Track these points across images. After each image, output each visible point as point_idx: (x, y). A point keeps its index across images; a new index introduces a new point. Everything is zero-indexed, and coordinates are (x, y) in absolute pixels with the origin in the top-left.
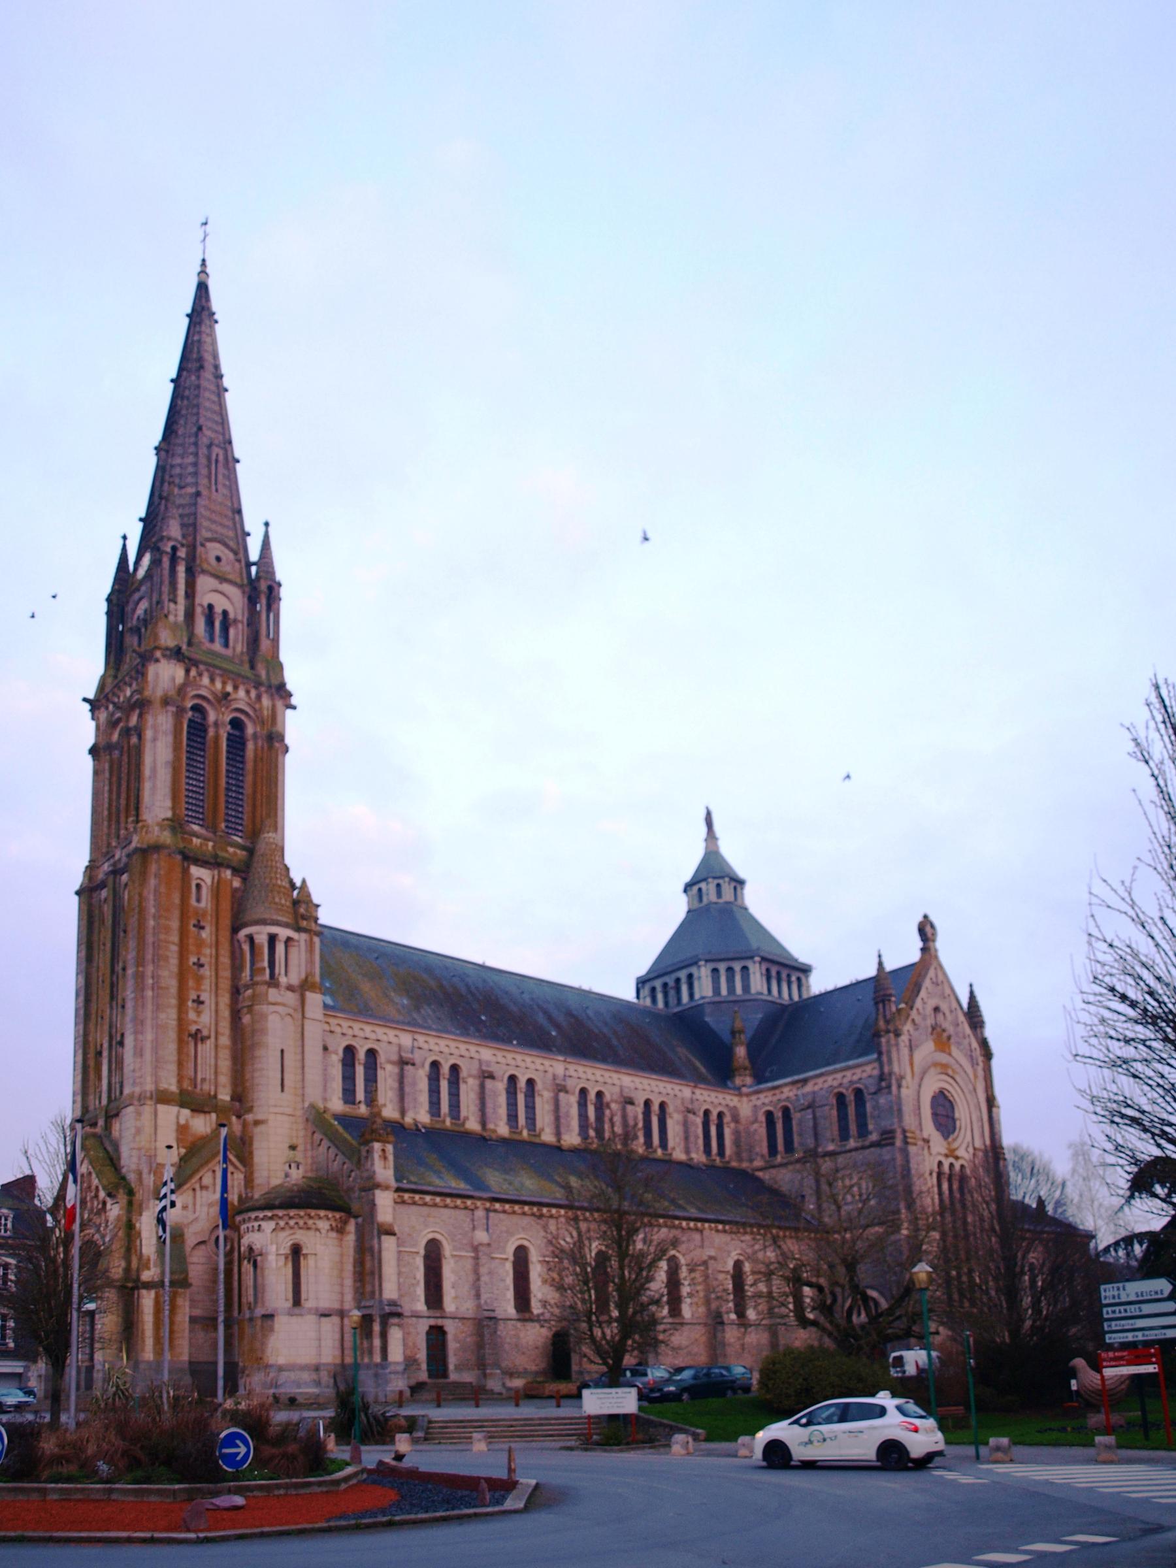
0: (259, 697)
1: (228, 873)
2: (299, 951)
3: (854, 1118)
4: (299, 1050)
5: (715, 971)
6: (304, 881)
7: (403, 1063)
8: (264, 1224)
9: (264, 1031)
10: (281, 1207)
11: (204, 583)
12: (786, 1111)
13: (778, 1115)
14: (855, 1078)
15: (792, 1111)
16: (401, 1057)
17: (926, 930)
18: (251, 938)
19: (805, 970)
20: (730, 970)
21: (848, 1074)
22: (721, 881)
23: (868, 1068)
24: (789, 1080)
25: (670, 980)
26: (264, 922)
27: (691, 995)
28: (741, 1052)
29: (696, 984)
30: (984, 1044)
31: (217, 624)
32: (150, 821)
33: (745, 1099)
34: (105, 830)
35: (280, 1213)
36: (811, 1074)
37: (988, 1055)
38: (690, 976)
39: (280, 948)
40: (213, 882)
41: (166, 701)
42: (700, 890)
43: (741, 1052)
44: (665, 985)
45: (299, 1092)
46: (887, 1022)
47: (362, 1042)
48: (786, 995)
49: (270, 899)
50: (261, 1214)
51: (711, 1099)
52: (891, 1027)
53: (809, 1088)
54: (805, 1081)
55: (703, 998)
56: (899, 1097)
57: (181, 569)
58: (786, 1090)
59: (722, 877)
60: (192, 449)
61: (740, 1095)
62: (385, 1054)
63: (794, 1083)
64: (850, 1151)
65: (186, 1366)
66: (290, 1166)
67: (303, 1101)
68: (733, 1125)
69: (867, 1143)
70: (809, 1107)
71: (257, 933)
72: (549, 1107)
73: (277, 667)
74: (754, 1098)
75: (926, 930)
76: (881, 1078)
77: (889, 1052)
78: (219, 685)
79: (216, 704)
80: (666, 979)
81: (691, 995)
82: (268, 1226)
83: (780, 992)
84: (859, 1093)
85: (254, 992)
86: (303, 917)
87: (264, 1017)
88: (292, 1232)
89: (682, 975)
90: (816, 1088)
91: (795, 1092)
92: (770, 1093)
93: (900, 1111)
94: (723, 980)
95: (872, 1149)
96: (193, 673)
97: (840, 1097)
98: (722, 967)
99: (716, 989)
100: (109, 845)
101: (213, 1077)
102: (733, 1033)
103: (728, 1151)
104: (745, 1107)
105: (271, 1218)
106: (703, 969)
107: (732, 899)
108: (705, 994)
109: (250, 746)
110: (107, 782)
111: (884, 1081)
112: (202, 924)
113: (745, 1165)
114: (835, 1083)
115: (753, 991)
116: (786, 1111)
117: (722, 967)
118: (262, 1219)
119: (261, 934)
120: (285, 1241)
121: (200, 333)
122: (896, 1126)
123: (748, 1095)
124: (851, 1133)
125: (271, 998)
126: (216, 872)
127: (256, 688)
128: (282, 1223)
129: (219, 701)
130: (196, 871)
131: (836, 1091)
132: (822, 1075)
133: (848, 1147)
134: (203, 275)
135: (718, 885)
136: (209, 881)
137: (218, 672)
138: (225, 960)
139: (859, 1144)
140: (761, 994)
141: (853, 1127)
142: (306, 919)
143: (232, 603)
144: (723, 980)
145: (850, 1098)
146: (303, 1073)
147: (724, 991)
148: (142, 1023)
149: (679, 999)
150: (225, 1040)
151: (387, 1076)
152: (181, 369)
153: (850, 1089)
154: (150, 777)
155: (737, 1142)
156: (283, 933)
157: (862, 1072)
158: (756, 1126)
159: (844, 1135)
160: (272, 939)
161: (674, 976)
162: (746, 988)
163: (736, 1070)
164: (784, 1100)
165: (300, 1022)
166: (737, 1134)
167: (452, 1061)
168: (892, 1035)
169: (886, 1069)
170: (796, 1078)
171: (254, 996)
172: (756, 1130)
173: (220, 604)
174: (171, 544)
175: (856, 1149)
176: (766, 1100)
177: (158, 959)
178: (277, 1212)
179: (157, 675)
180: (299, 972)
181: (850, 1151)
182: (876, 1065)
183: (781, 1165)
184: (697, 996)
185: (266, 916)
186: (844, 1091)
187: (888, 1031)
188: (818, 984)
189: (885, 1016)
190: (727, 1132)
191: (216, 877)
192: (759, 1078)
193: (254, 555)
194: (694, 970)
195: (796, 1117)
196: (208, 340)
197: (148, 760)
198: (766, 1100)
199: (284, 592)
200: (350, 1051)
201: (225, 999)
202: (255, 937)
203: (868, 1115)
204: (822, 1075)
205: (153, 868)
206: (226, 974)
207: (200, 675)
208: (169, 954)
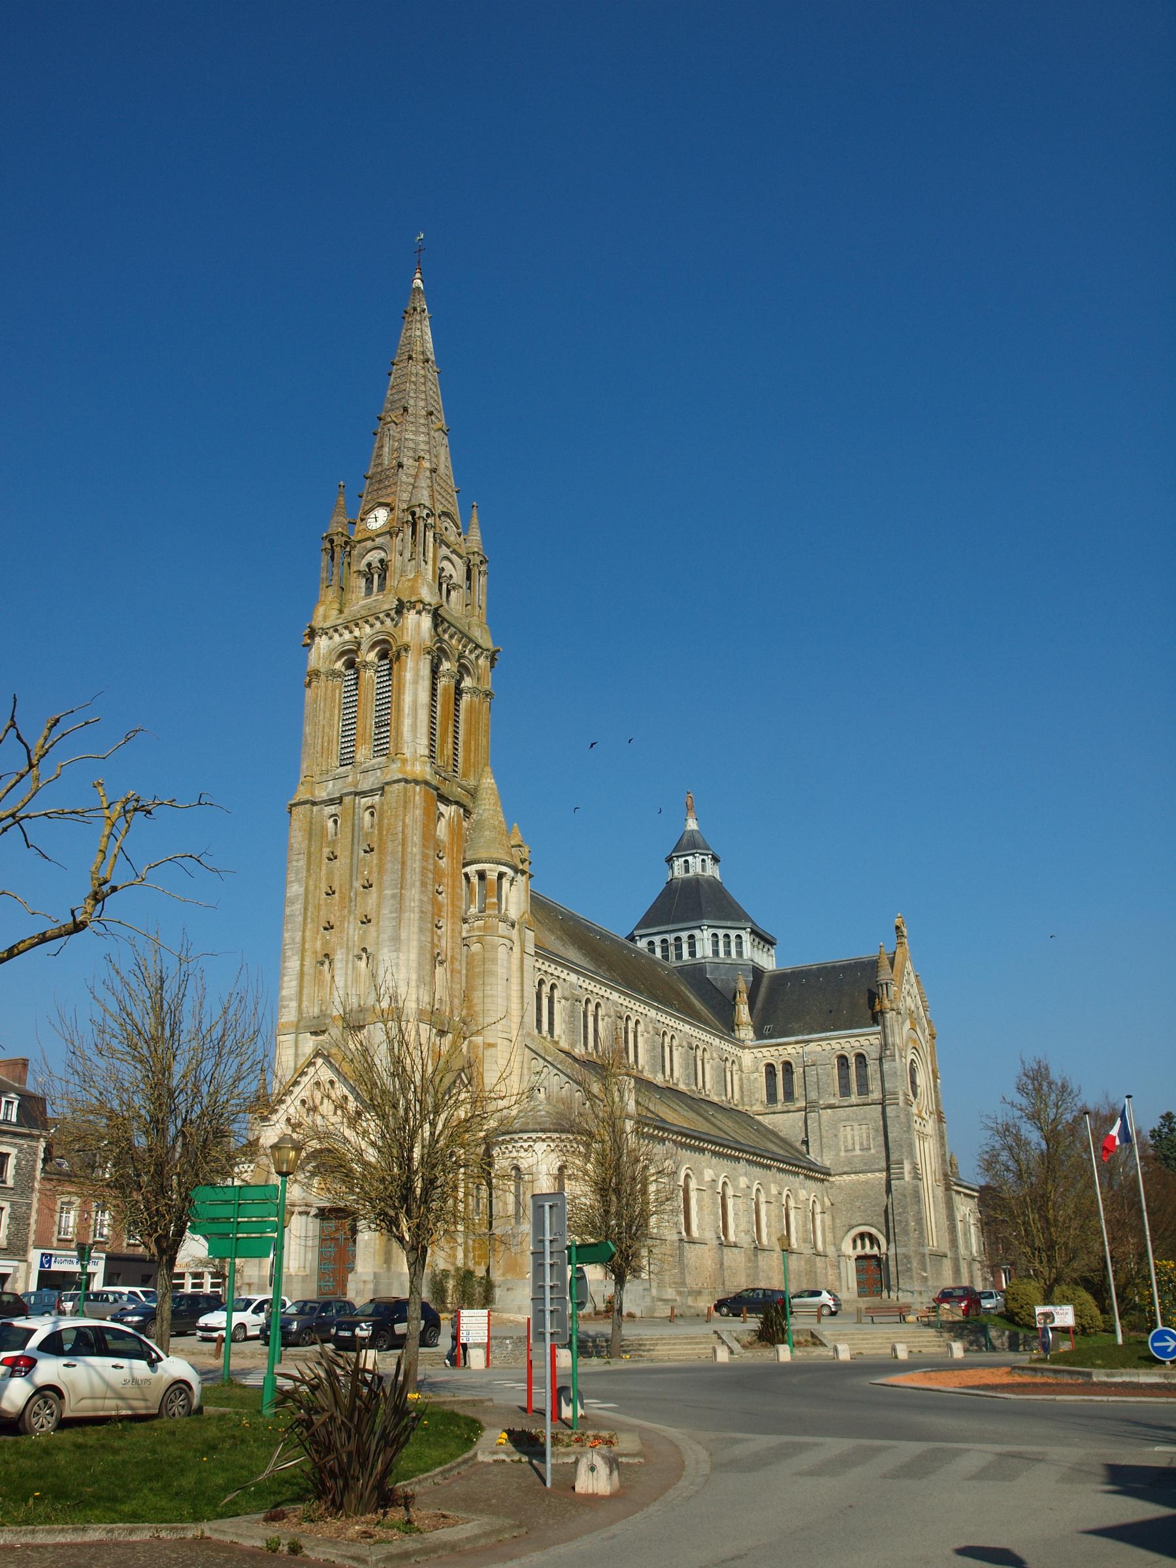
5: (715, 935)
12: (787, 1066)
15: (794, 1066)
20: (727, 936)
22: (705, 857)
27: (692, 954)
29: (698, 945)
35: (555, 1135)
38: (691, 937)
42: (686, 862)
50: (534, 1135)
54: (808, 1042)
55: (704, 958)
58: (789, 1048)
81: (692, 954)
89: (684, 935)
97: (843, 1059)
98: (721, 933)
105: (544, 1140)
108: (706, 955)
115: (745, 957)
116: (787, 1066)
131: (839, 1053)
135: (703, 860)
139: (859, 1101)
145: (852, 1060)
147: (722, 954)
149: (679, 956)
159: (845, 1090)
162: (740, 954)
166: (741, 1079)
170: (800, 1038)
178: (549, 1135)
184: (698, 955)
186: (846, 1054)
194: (696, 932)
195: (798, 1071)
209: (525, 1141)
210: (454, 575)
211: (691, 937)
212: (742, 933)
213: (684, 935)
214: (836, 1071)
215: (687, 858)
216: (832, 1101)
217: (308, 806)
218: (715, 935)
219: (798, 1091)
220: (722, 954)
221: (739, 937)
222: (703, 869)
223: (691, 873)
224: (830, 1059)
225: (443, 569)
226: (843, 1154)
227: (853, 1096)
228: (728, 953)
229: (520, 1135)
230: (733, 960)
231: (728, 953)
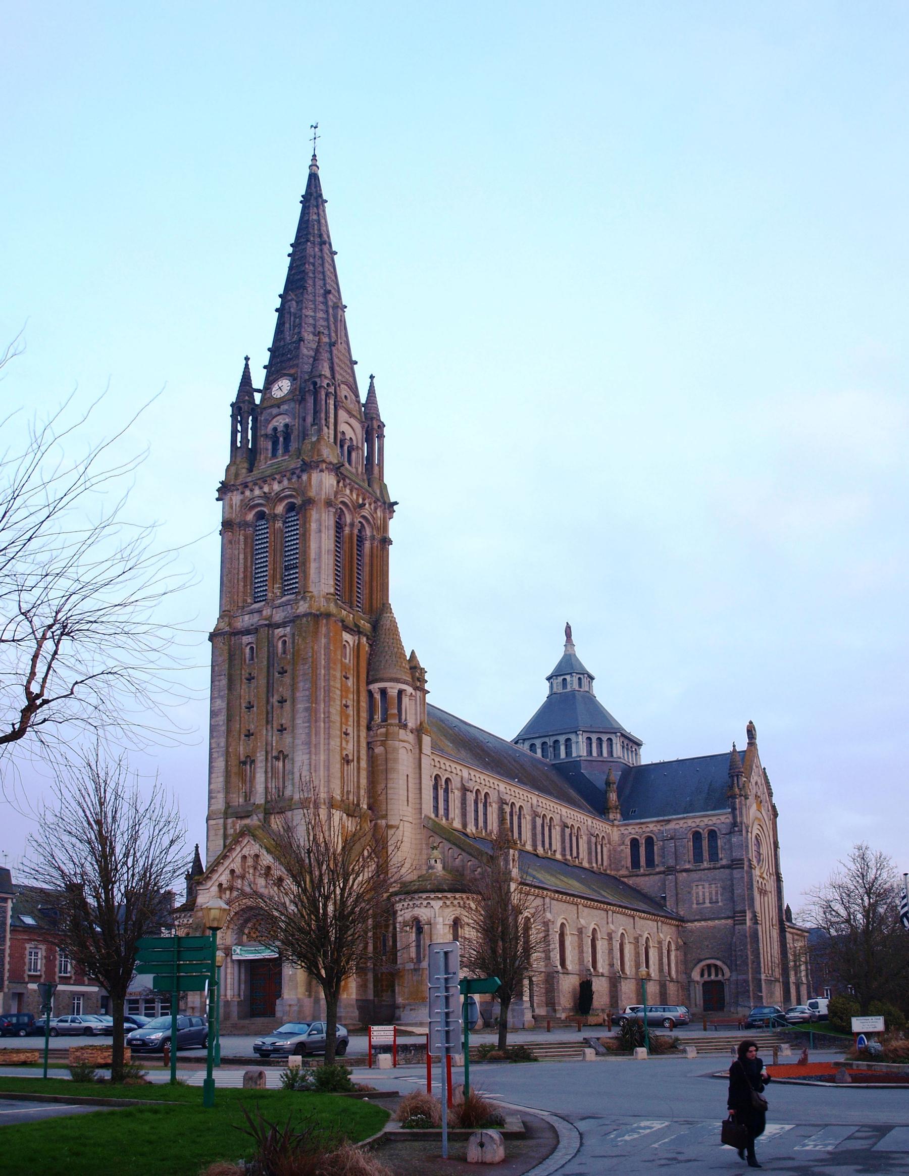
0: (376, 509)
1: (365, 639)
2: (416, 704)
3: (707, 848)
4: (417, 775)
5: (589, 739)
6: (413, 652)
7: (464, 790)
8: (433, 903)
9: (396, 760)
10: (450, 891)
11: (342, 414)
13: (643, 841)
14: (710, 823)
16: (463, 785)
17: (751, 732)
18: (383, 692)
19: (639, 744)
21: (706, 820)
23: (723, 818)
24: (655, 819)
25: (550, 741)
26: (397, 680)
27: (569, 753)
28: (613, 796)
29: (574, 746)
30: (774, 807)
31: (346, 448)
32: (315, 593)
33: (615, 828)
34: (241, 589)
35: (449, 895)
36: (674, 817)
37: (776, 815)
38: (568, 740)
39: (405, 701)
40: (354, 645)
41: (329, 504)
43: (613, 796)
44: (544, 744)
45: (418, 806)
46: (740, 789)
47: (444, 772)
48: (630, 760)
49: (399, 663)
50: (432, 896)
51: (599, 826)
52: (743, 793)
53: (672, 826)
54: (669, 821)
56: (747, 838)
57: (332, 402)
58: (651, 826)
59: (583, 674)
60: (322, 307)
61: (613, 826)
62: (456, 783)
63: (658, 822)
64: (704, 870)
65: (354, 1002)
66: (436, 861)
67: (421, 813)
68: (608, 845)
69: (718, 865)
70: (672, 839)
71: (391, 688)
72: (529, 826)
73: (383, 488)
74: (622, 829)
75: (751, 732)
76: (734, 824)
77: (741, 809)
78: (355, 496)
79: (352, 509)
80: (546, 740)
81: (569, 753)
82: (436, 905)
83: (628, 758)
84: (712, 834)
85: (387, 731)
86: (418, 680)
87: (395, 750)
88: (454, 908)
89: (562, 739)
90: (677, 827)
91: (659, 827)
92: (637, 827)
93: (747, 846)
94: (594, 746)
95: (722, 870)
96: (341, 484)
97: (697, 836)
99: (590, 753)
100: (245, 601)
101: (356, 790)
102: (608, 783)
103: (605, 863)
104: (615, 835)
105: (440, 899)
106: (580, 737)
107: (588, 690)
109: (367, 544)
110: (242, 551)
111: (736, 827)
112: (348, 676)
113: (613, 873)
114: (694, 825)
115: (615, 755)
116: (650, 841)
117: (594, 737)
118: (432, 899)
119: (393, 689)
120: (449, 915)
121: (309, 213)
122: (744, 857)
123: (618, 826)
124: (704, 858)
125: (401, 737)
126: (357, 638)
127: (375, 502)
128: (448, 902)
129: (355, 509)
130: (346, 636)
131: (694, 829)
132: (684, 818)
133: (702, 867)
134: (315, 168)
136: (351, 643)
137: (356, 486)
138: (364, 704)
140: (620, 758)
141: (706, 855)
142: (420, 681)
143: (355, 434)
144: (594, 746)
146: (421, 793)
147: (595, 754)
148: (317, 746)
150: (363, 764)
151: (455, 796)
152: (297, 238)
153: (706, 830)
154: (315, 559)
155: (609, 857)
156: (409, 690)
157: (719, 819)
158: (622, 847)
159: (698, 857)
160: (400, 692)
161: (555, 738)
162: (611, 753)
163: (611, 808)
164: (648, 832)
165: (417, 756)
167: (486, 791)
168: (743, 798)
169: (738, 820)
171: (387, 735)
172: (622, 850)
173: (349, 434)
174: (326, 381)
175: (709, 869)
176: (633, 830)
177: (328, 700)
178: (446, 894)
179: (321, 483)
180: (416, 719)
181: (704, 870)
182: (730, 816)
183: (643, 875)
184: (574, 755)
185: (399, 676)
187: (741, 795)
188: (648, 756)
189: (738, 786)
190: (605, 849)
191: (356, 642)
192: (626, 816)
193: (363, 400)
196: (323, 221)
197: (313, 546)
198: (633, 830)
199: (386, 431)
200: (437, 777)
201: (363, 733)
202: (389, 690)
203: (719, 847)
204: (684, 818)
205: (323, 630)
206: (364, 715)
207: (345, 487)
208: (335, 696)
209: (425, 899)
210: (354, 438)
211: (568, 740)
212: (613, 737)
213: (562, 739)
214: (691, 844)
215: (565, 677)
216: (687, 866)
218: (589, 739)
219: (657, 859)
220: (595, 754)
221: (610, 740)
222: (580, 685)
223: (569, 689)
224: (687, 834)
225: (343, 433)
226: (695, 906)
227: (705, 863)
228: (600, 753)
229: (420, 895)
230: (605, 758)
231: (600, 753)
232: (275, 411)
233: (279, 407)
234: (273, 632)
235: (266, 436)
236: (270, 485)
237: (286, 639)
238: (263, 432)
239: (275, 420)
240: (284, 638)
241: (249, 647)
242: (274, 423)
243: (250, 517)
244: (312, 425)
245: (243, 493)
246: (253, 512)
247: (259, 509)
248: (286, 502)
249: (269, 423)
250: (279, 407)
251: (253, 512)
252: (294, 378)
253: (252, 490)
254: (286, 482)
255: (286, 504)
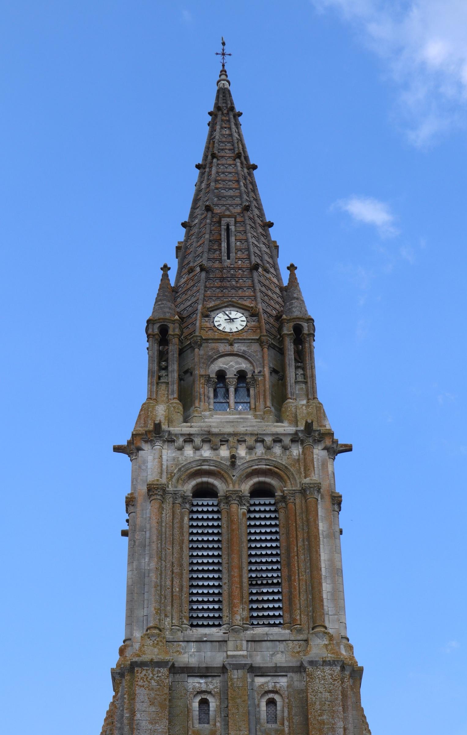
217: (164, 671)
232: (223, 348)
233: (231, 345)
234: (253, 681)
235: (208, 379)
236: (230, 448)
237: (277, 697)
238: (202, 372)
239: (221, 360)
240: (271, 696)
241: (198, 699)
242: (220, 364)
243: (189, 487)
244: (296, 382)
245: (180, 449)
246: (193, 483)
247: (205, 479)
248: (256, 480)
249: (212, 362)
250: (231, 345)
251: (193, 483)
252: (252, 313)
253: (197, 449)
254: (260, 450)
255: (255, 484)
